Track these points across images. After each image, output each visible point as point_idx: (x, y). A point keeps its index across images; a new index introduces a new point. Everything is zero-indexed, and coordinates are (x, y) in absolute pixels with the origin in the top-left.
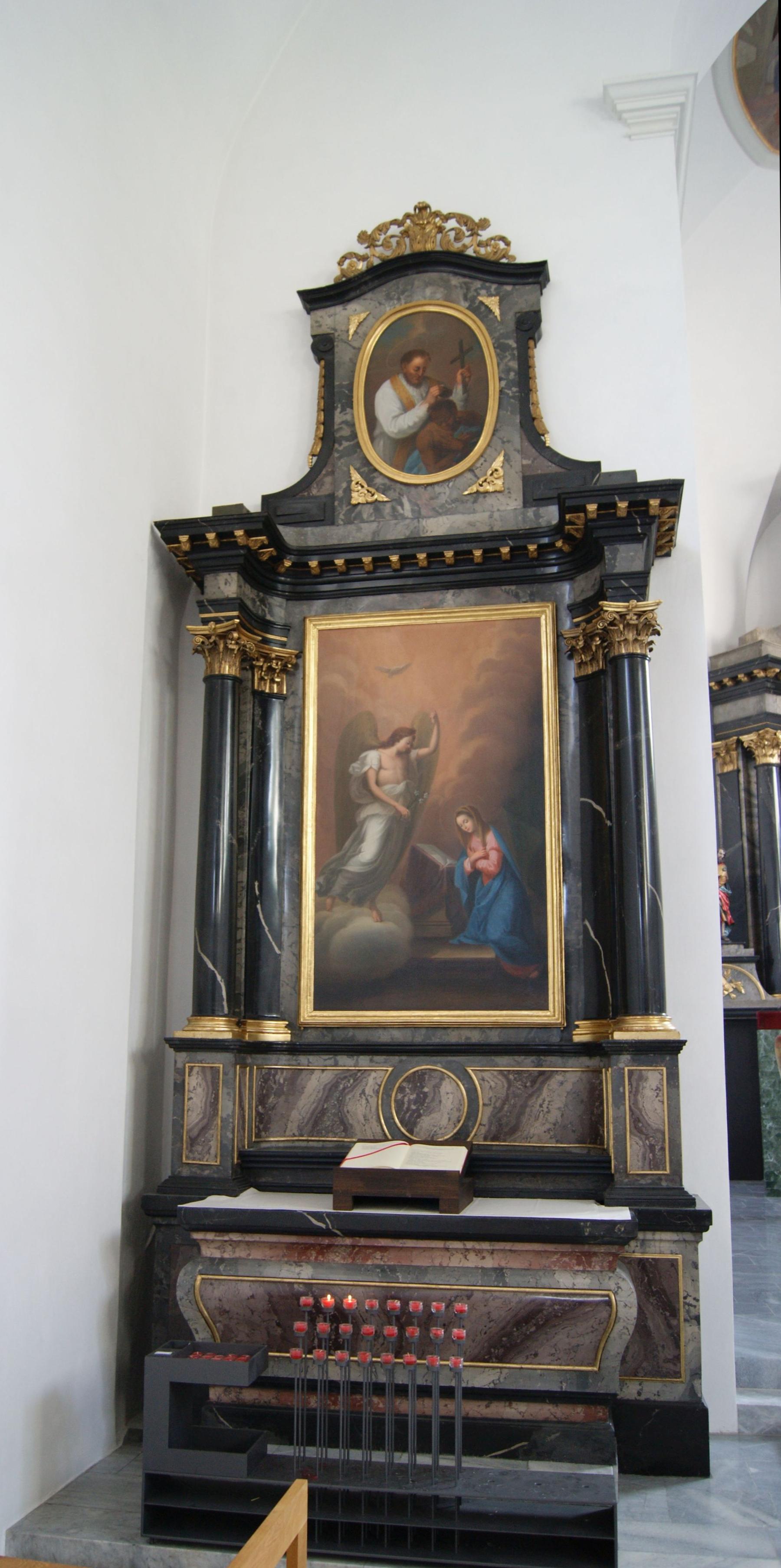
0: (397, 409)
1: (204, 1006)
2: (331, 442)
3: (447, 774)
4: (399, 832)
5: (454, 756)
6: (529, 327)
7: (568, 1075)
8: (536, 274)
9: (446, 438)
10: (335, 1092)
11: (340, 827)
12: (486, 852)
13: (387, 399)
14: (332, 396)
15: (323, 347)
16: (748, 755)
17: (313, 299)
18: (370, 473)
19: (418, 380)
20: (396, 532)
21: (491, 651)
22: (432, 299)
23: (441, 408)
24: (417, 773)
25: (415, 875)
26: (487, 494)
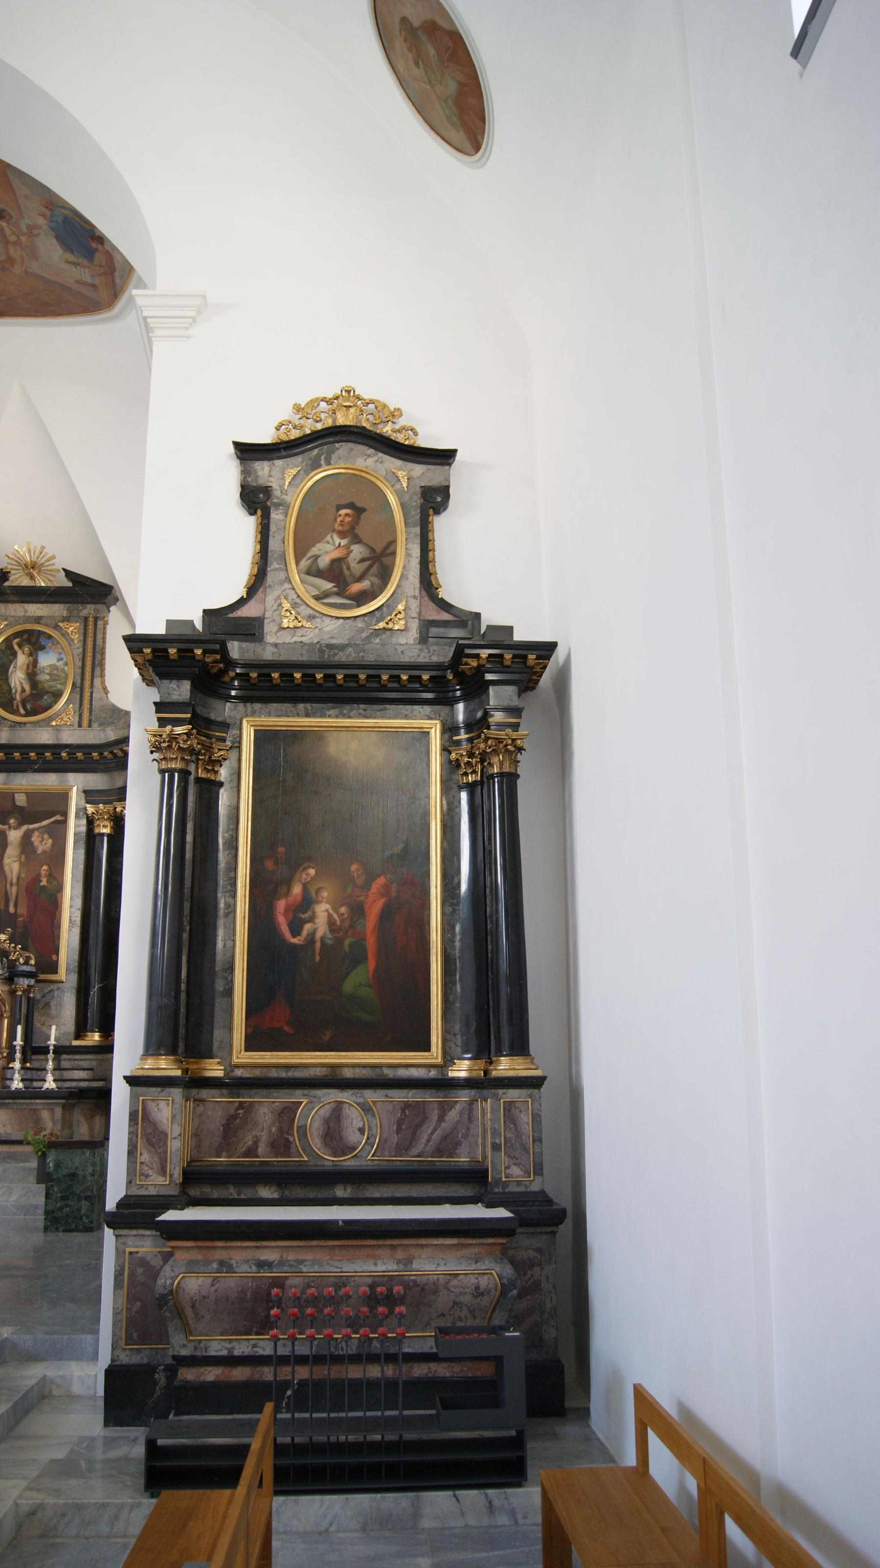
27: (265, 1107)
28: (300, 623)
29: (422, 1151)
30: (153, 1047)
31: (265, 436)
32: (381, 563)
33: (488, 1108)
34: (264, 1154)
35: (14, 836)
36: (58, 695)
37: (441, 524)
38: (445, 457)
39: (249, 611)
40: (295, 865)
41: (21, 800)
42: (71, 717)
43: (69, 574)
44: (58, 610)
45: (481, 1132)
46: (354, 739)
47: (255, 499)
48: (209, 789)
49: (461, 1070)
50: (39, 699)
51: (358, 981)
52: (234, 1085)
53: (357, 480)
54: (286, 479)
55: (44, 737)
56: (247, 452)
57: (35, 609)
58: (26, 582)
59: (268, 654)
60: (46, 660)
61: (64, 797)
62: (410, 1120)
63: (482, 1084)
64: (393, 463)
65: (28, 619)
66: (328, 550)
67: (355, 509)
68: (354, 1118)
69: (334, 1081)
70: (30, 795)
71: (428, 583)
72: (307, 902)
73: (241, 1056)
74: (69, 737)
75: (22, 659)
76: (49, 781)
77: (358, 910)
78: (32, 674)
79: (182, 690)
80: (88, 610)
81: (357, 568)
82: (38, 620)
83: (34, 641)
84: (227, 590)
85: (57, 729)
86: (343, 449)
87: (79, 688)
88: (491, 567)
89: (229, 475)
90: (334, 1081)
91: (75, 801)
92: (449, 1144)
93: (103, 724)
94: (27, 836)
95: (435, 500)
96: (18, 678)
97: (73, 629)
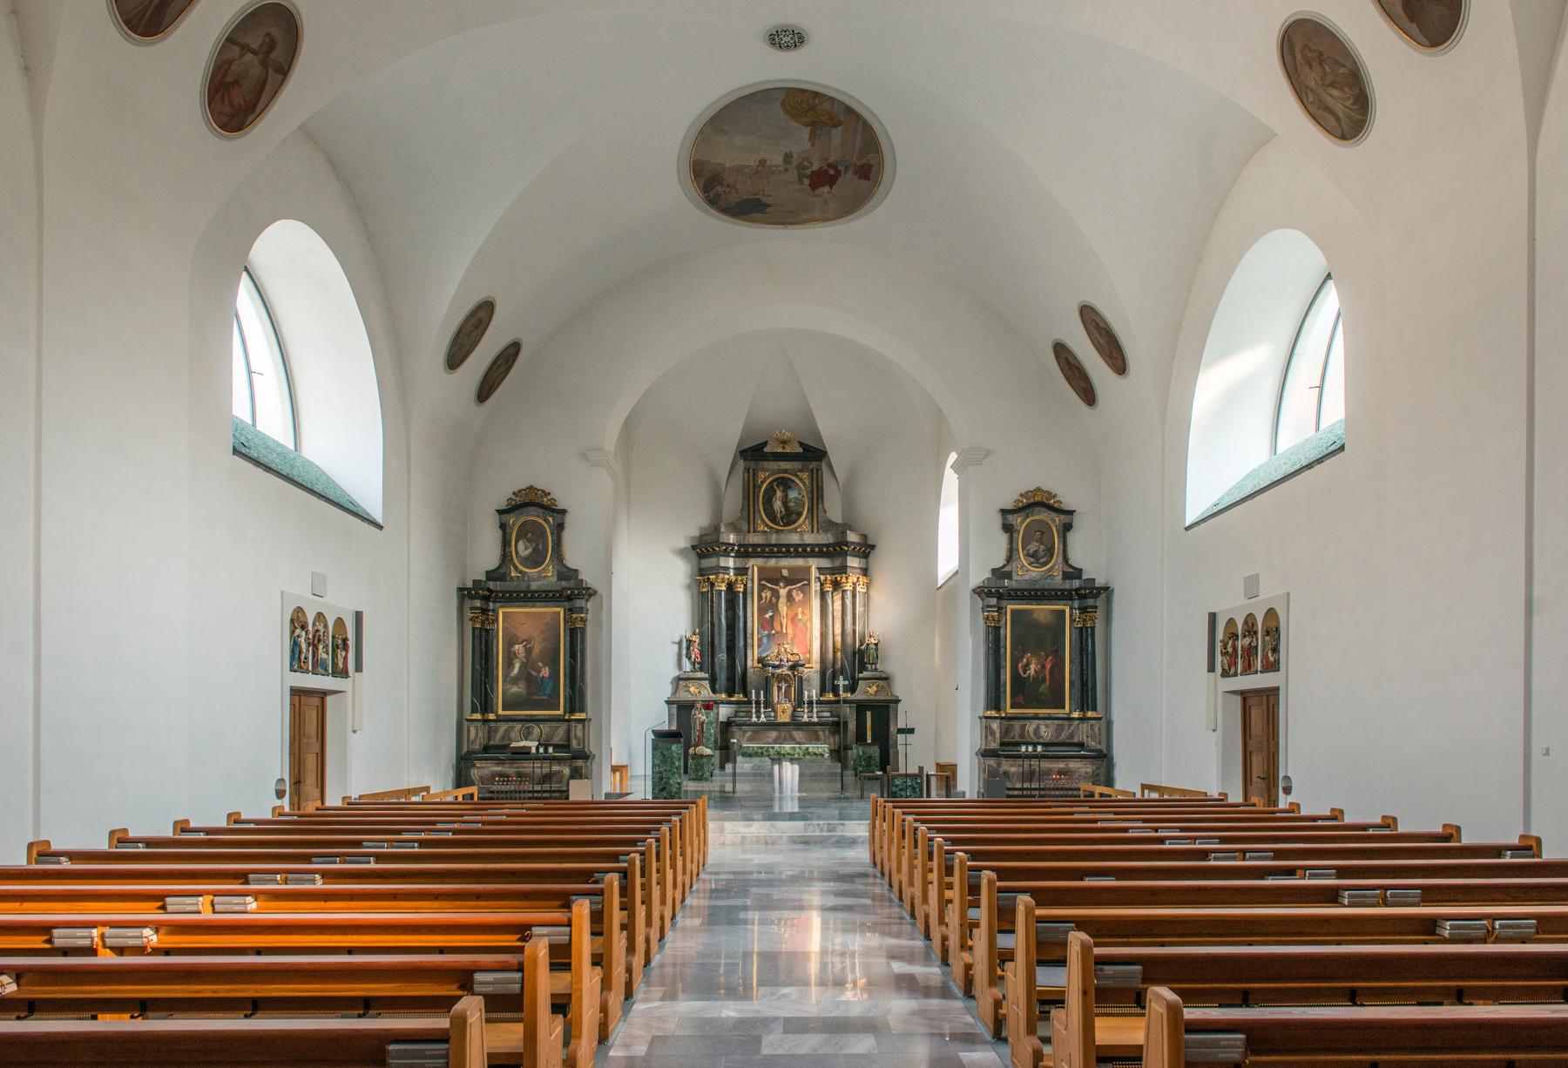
0: (523, 549)
1: (474, 711)
2: (505, 557)
3: (536, 652)
4: (524, 666)
5: (537, 649)
6: (560, 527)
7: (564, 726)
8: (564, 512)
9: (535, 560)
10: (507, 731)
11: (509, 665)
12: (545, 672)
13: (521, 545)
14: (506, 543)
15: (503, 526)
16: (712, 585)
17: (500, 512)
18: (516, 568)
19: (529, 541)
20: (523, 587)
21: (548, 619)
22: (534, 516)
23: (535, 550)
24: (528, 651)
25: (527, 676)
26: (545, 576)
27: (1017, 725)
28: (1026, 573)
29: (1063, 737)
30: (988, 708)
31: (1009, 506)
32: (1050, 551)
33: (1085, 726)
34: (1017, 739)
35: (783, 592)
36: (800, 514)
37: (1070, 535)
38: (1071, 513)
39: (1007, 569)
40: (1024, 652)
41: (785, 573)
42: (807, 527)
43: (801, 444)
44: (796, 465)
45: (1083, 733)
46: (1042, 611)
47: (1008, 528)
48: (997, 629)
49: (1076, 715)
50: (790, 517)
51: (1043, 688)
52: (1008, 718)
53: (1041, 521)
54: (1016, 520)
55: (794, 539)
56: (1004, 512)
57: (784, 465)
58: (780, 450)
59: (1014, 585)
60: (792, 494)
61: (808, 569)
62: (1060, 729)
63: (1083, 719)
64: (1053, 515)
65: (780, 471)
66: (1033, 547)
67: (1042, 532)
68: (1043, 728)
69: (1036, 717)
70: (790, 569)
71: (1065, 559)
72: (1028, 664)
73: (1010, 711)
74: (809, 539)
75: (779, 494)
76: (800, 562)
77: (1043, 667)
78: (785, 503)
79: (994, 601)
80: (813, 465)
81: (1041, 553)
82: (786, 471)
83: (786, 484)
84: (999, 561)
85: (801, 533)
86: (1037, 509)
87: (811, 510)
88: (1086, 552)
89: (997, 521)
90: (1036, 717)
91: (814, 573)
92: (1072, 736)
93: (826, 531)
94: (790, 593)
95: (1068, 527)
96: (778, 505)
97: (805, 476)
